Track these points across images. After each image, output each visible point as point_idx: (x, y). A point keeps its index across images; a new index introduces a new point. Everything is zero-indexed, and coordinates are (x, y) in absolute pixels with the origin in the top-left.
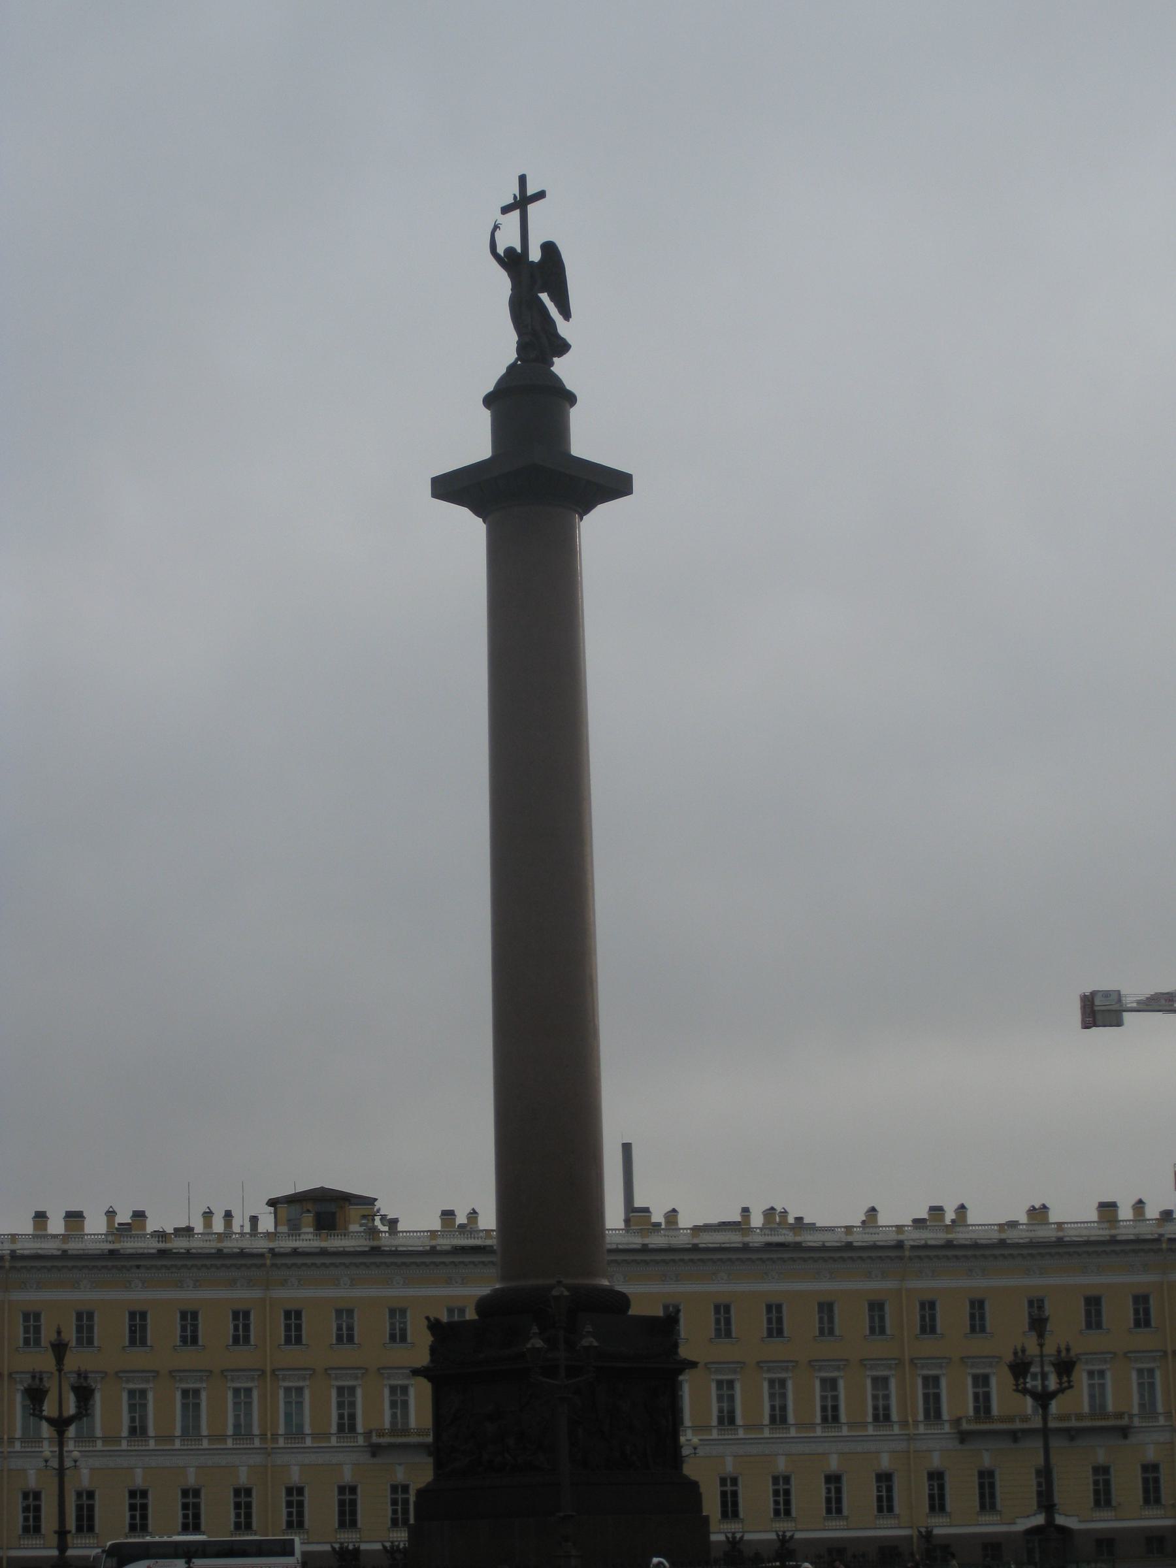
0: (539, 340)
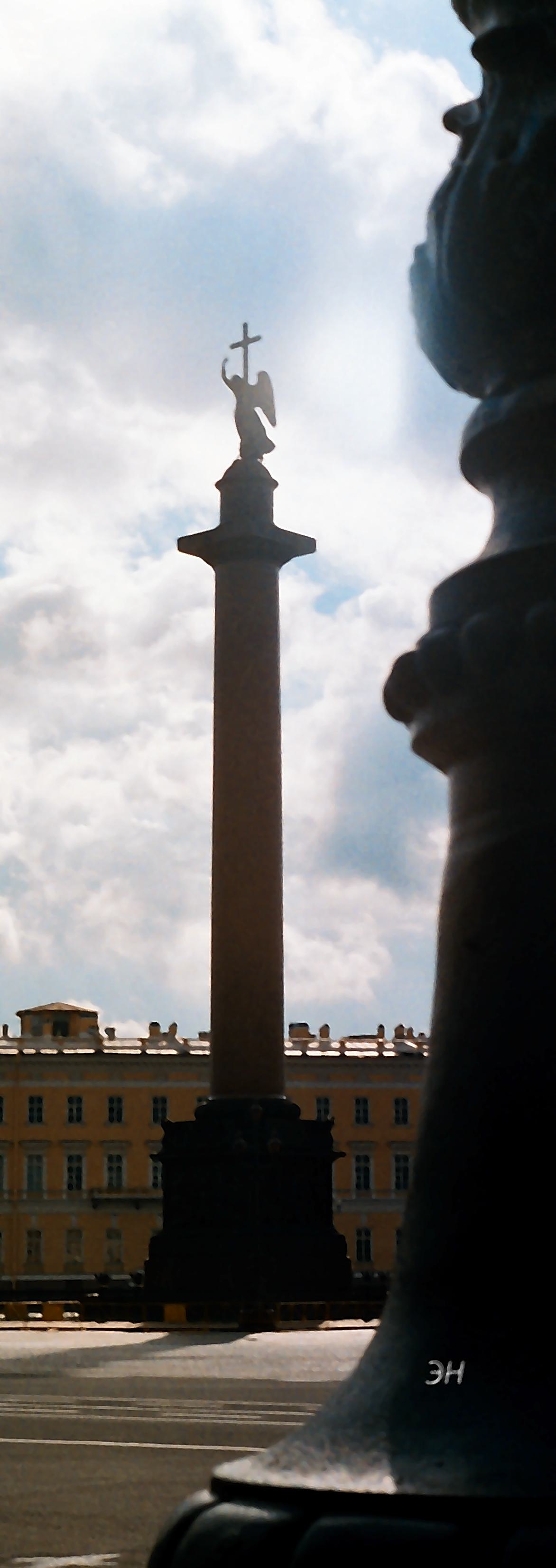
0: (254, 443)
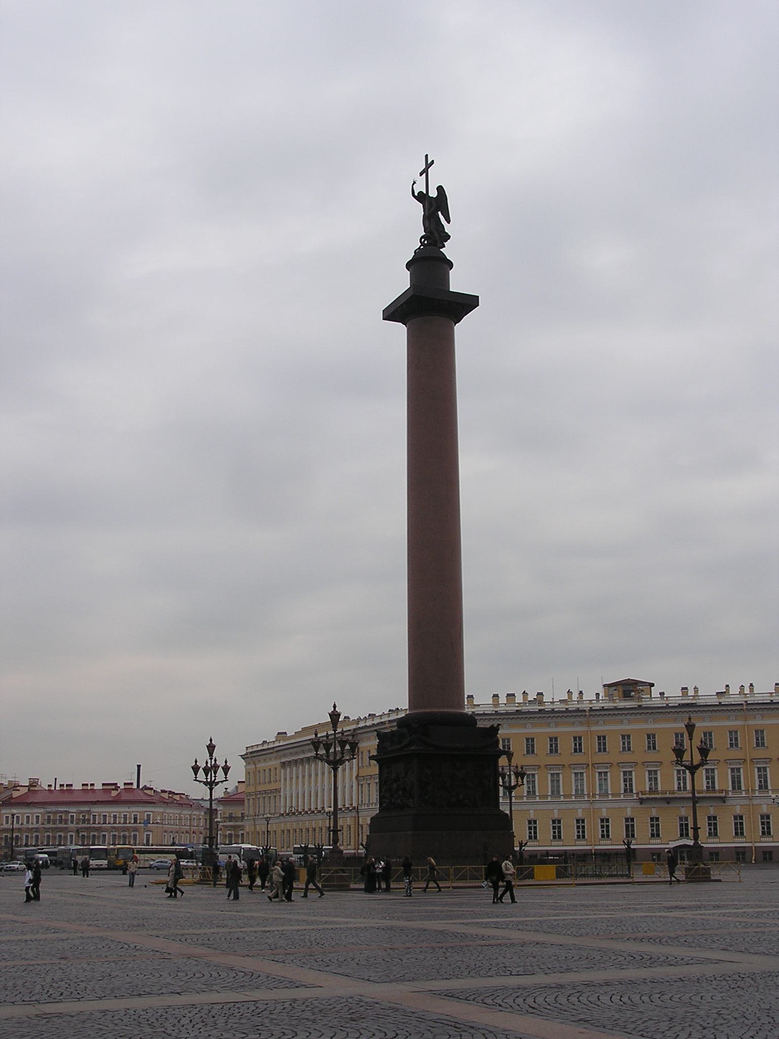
0: (435, 235)
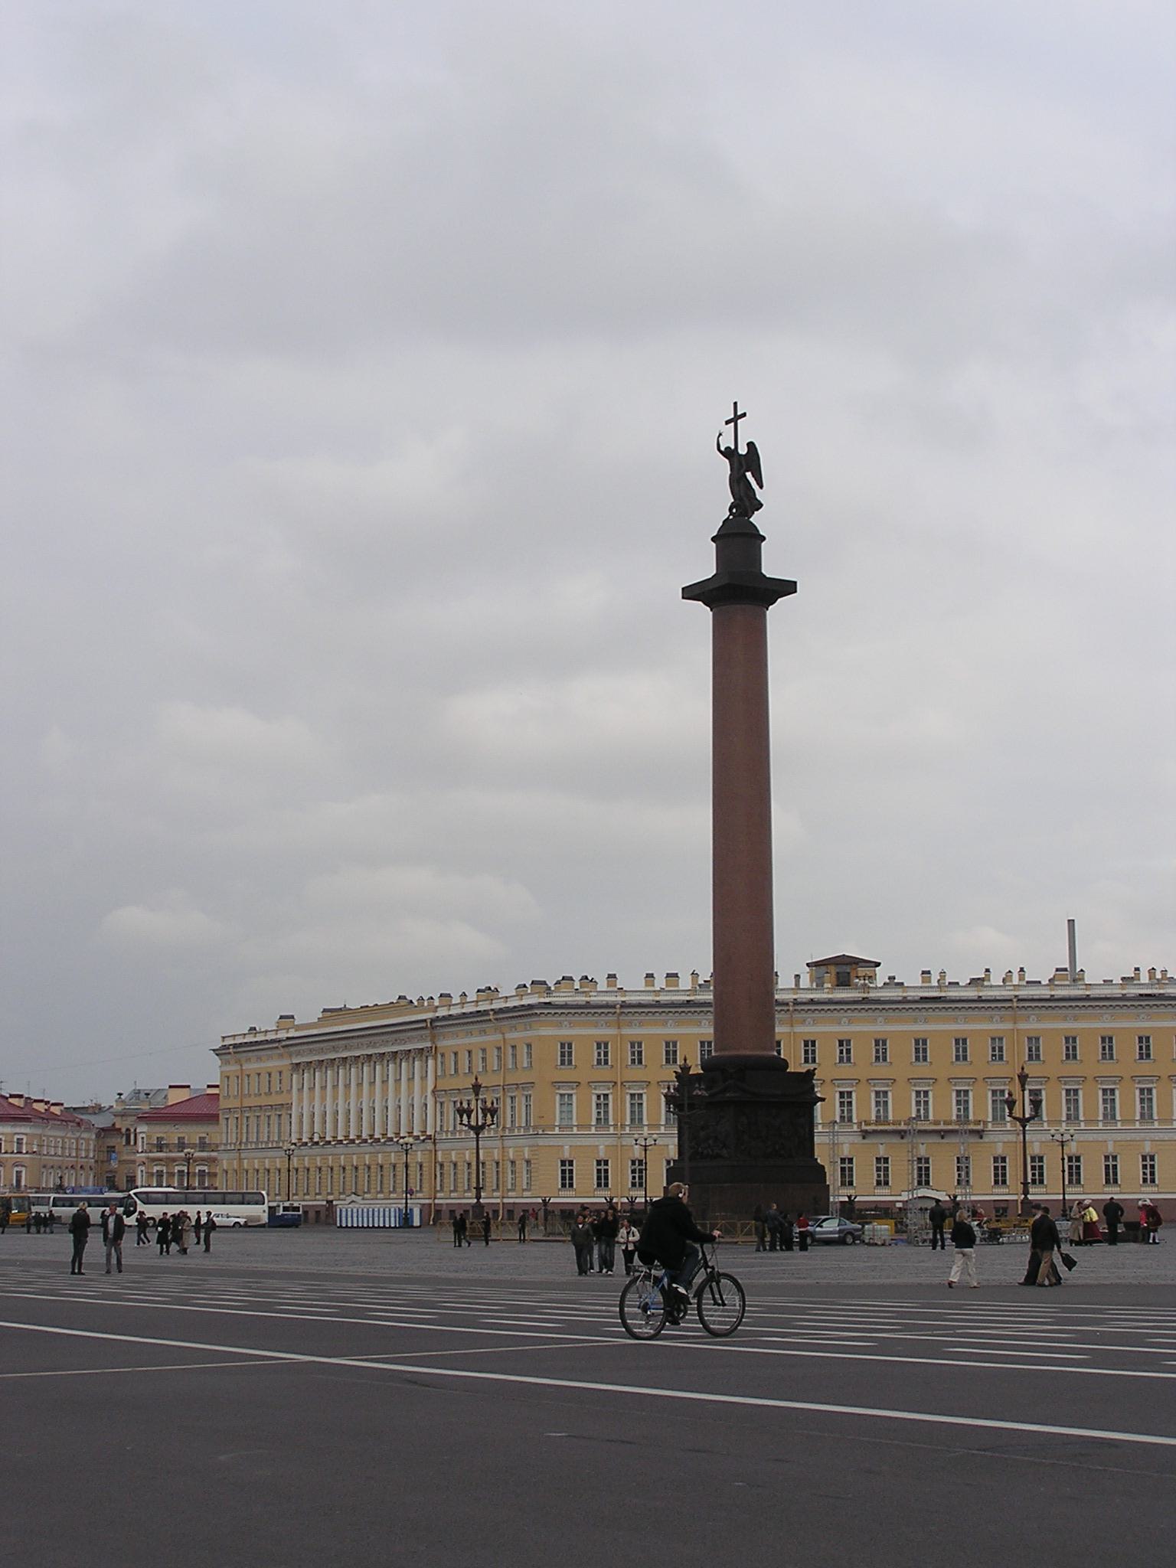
0: (745, 502)
